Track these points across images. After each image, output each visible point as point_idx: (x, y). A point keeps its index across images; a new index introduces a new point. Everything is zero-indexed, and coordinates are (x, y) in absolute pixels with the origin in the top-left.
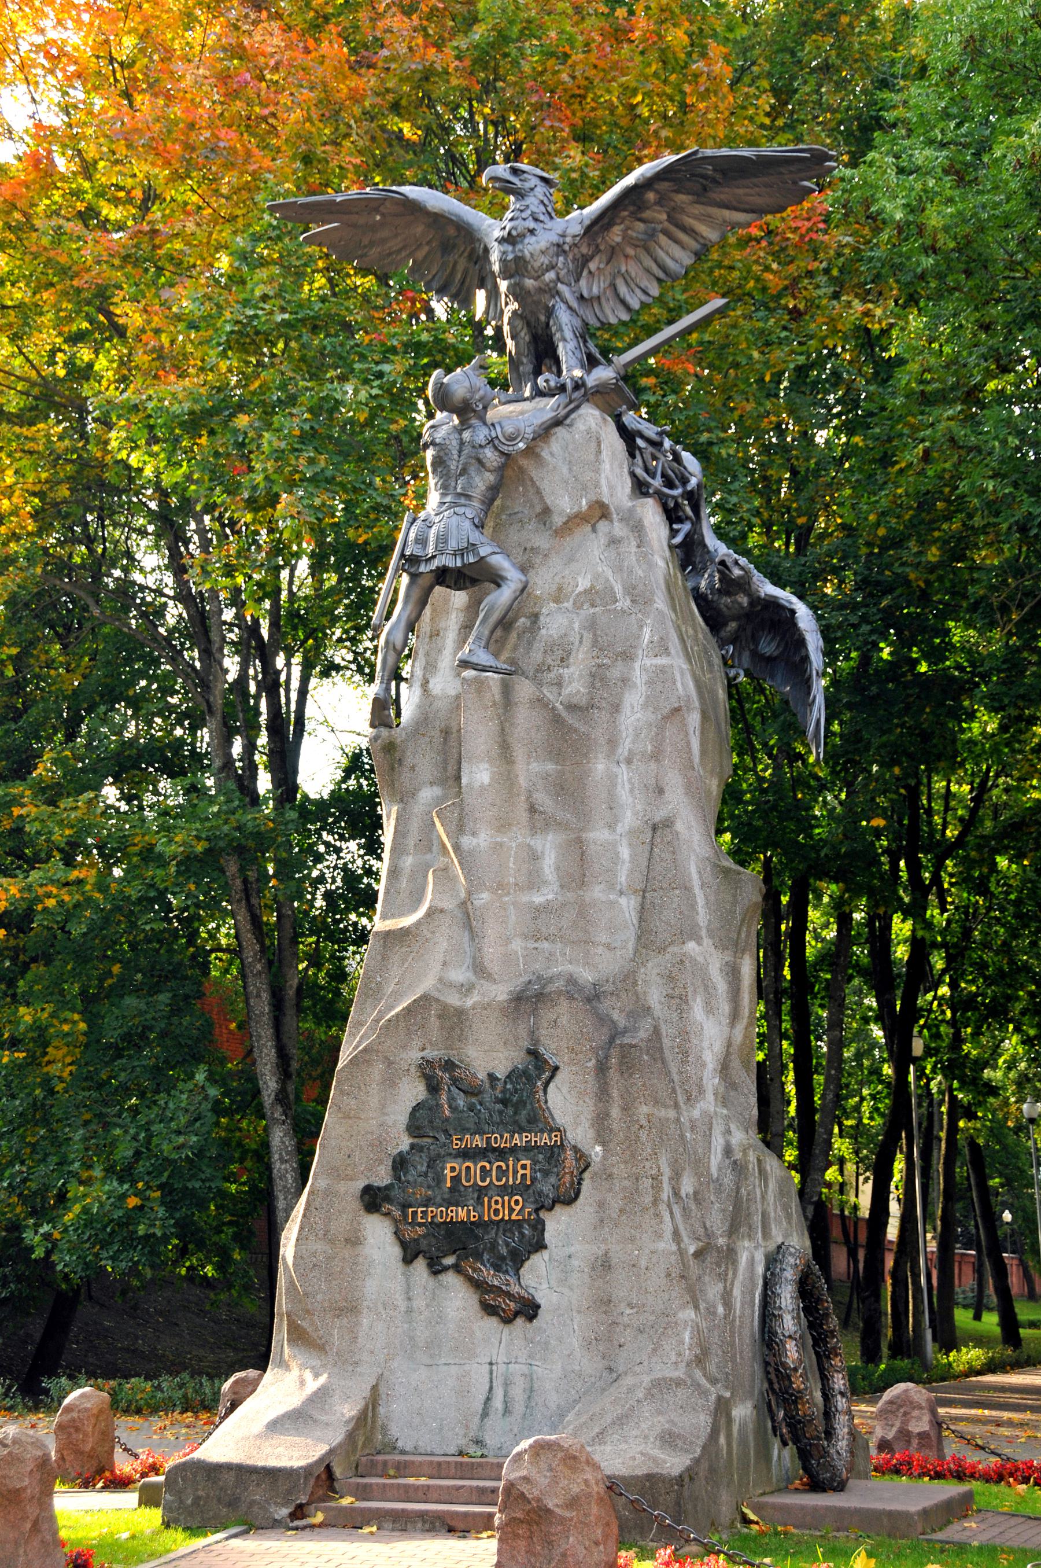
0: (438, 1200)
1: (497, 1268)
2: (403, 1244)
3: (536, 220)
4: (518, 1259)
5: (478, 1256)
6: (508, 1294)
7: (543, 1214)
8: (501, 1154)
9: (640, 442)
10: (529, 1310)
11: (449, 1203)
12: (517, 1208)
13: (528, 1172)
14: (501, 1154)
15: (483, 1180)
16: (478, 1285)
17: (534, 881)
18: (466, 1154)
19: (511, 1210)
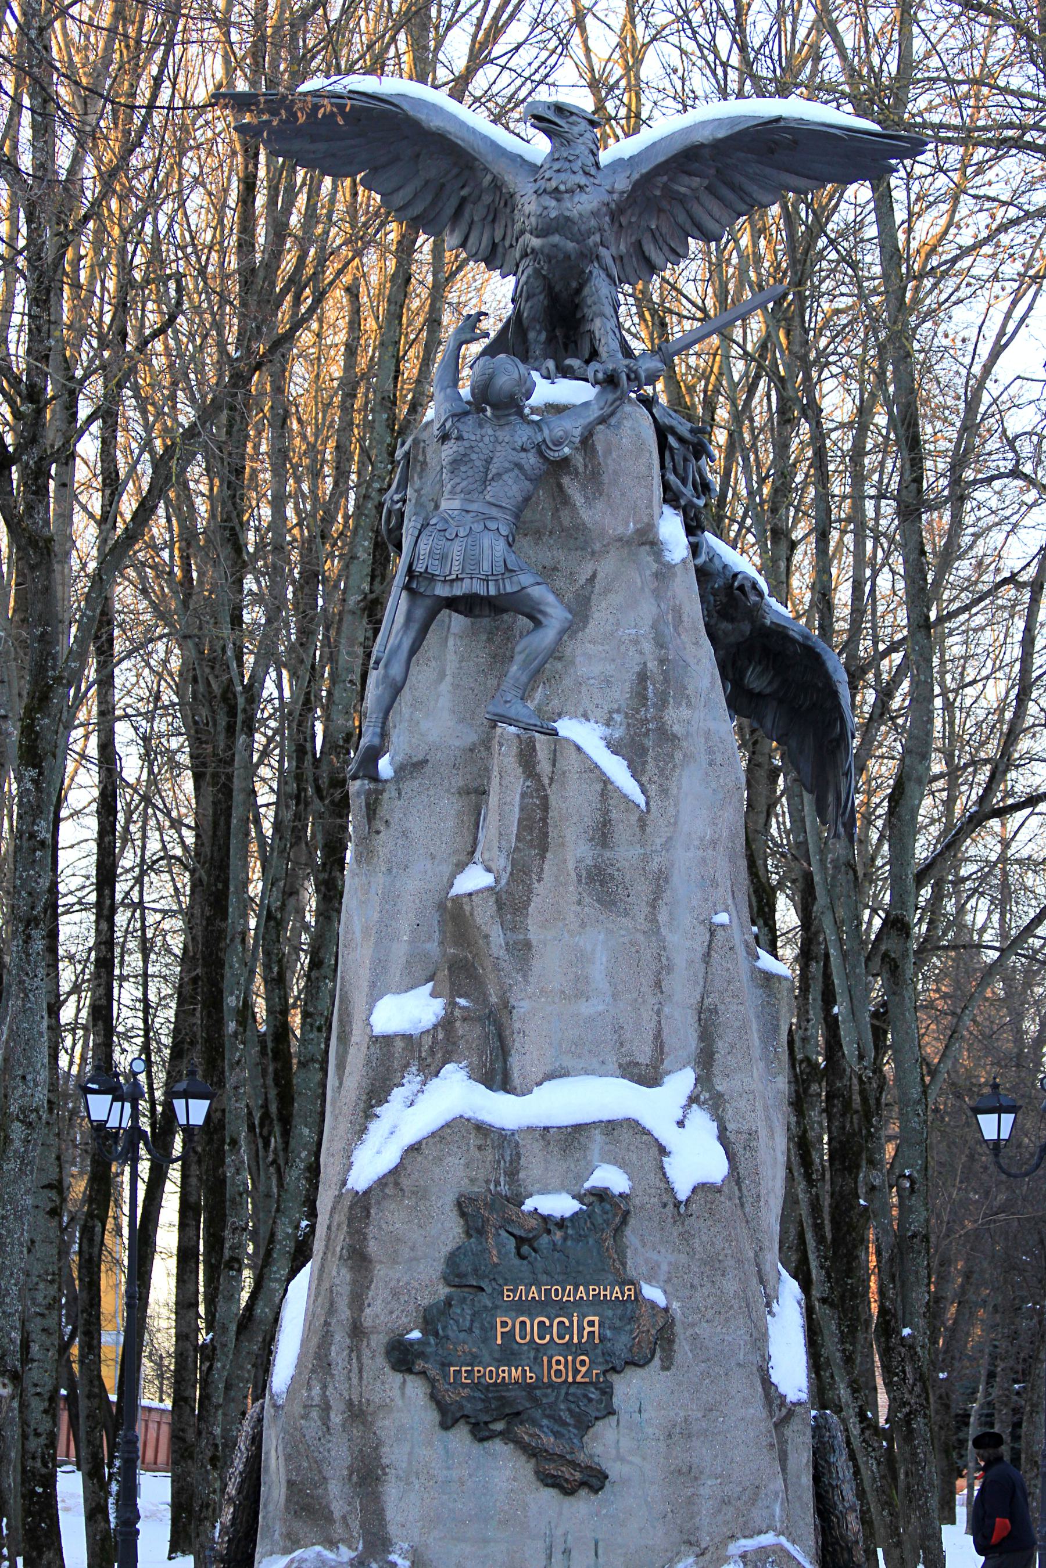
0: (487, 1358)
1: (557, 1435)
2: (442, 1407)
3: (586, 173)
4: (584, 1425)
5: (534, 1423)
6: (574, 1465)
7: (614, 1378)
8: (563, 1308)
9: (672, 440)
10: (594, 1480)
11: (499, 1362)
12: (585, 1368)
13: (596, 1329)
14: (563, 1308)
15: (541, 1338)
16: (532, 1452)
17: (580, 989)
18: (522, 1307)
19: (576, 1372)
